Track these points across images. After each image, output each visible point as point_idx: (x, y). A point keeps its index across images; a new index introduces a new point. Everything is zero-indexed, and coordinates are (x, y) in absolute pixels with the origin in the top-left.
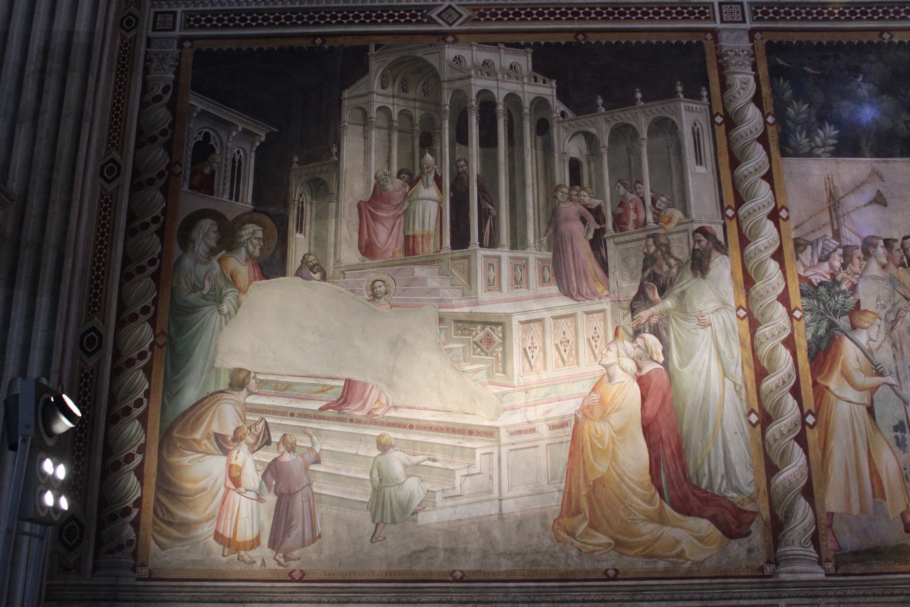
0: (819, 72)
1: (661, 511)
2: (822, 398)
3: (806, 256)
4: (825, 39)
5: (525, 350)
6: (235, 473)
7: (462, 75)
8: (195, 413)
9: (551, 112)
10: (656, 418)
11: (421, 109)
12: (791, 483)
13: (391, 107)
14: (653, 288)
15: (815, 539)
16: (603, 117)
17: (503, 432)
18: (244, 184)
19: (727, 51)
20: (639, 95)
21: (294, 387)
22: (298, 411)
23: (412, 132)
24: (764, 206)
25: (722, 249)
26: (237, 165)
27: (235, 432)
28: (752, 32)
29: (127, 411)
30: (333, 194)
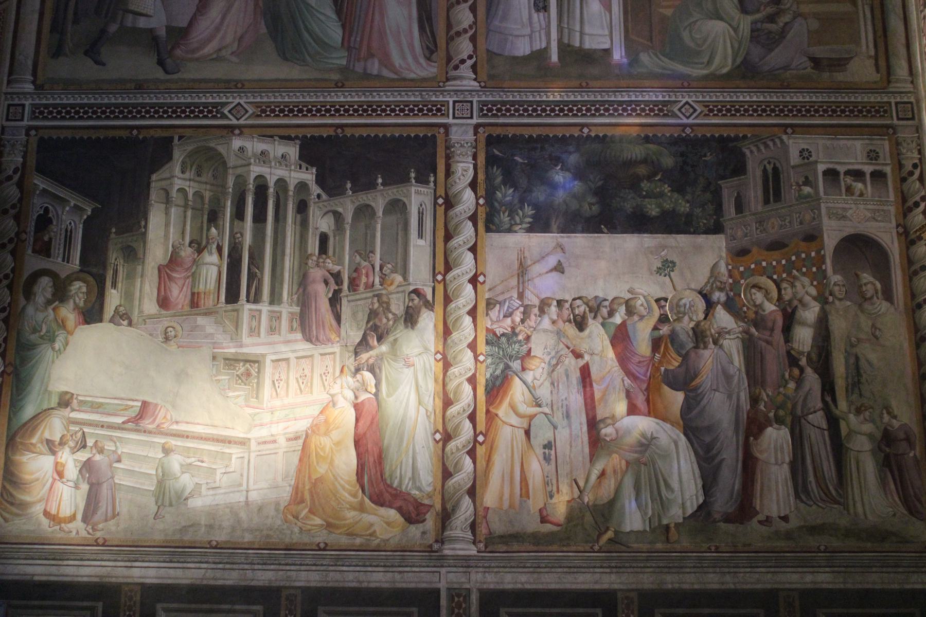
3: (494, 313)
4: (535, 132)
5: (273, 381)
6: (59, 468)
7: (244, 162)
9: (310, 195)
10: (365, 434)
12: (459, 485)
13: (187, 189)
14: (373, 336)
15: (473, 526)
20: (380, 181)
23: (202, 210)
25: (430, 306)
26: (69, 234)
27: (61, 438)
28: (477, 127)
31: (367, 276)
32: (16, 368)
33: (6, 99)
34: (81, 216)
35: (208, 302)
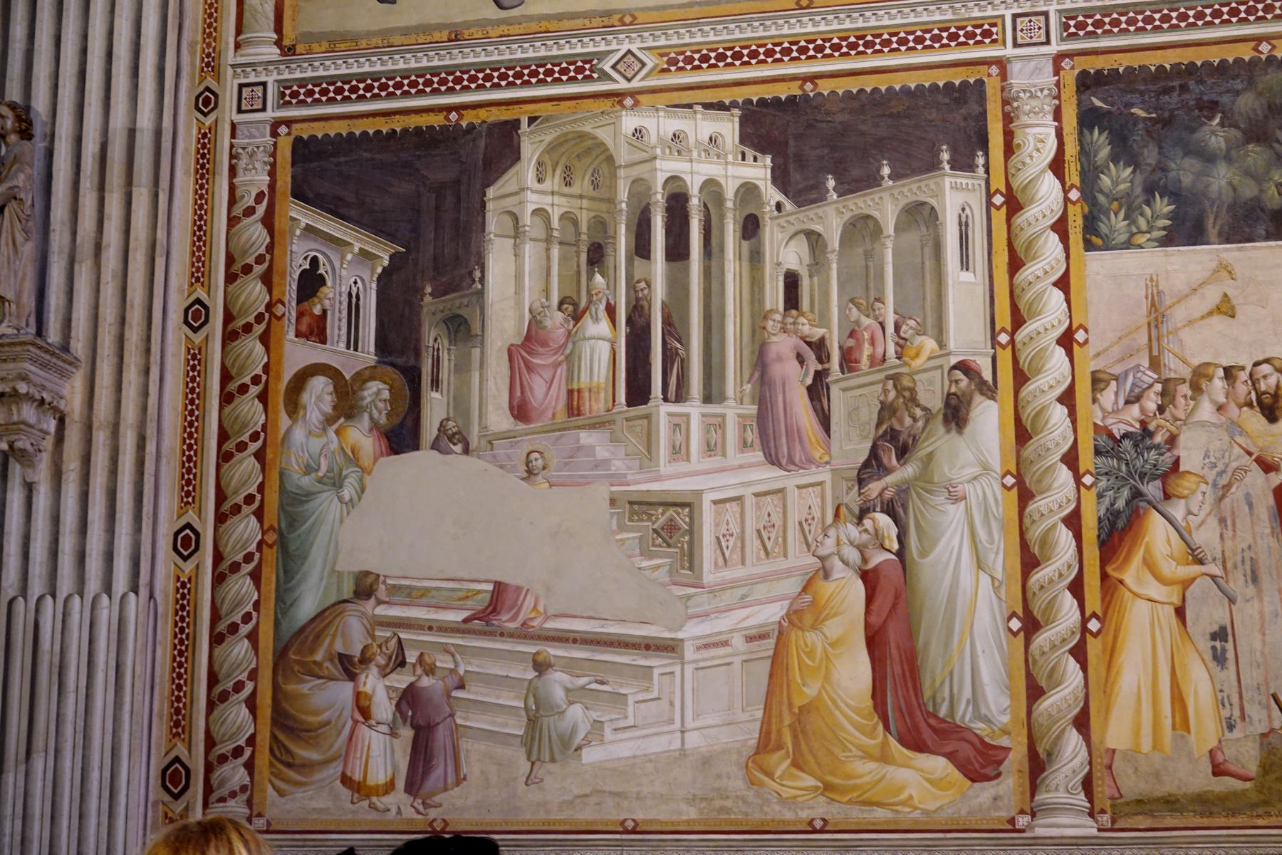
0: (1154, 115)
1: (885, 743)
2: (1112, 595)
3: (1108, 397)
4: (1168, 59)
5: (718, 538)
6: (364, 703)
7: (644, 155)
8: (314, 629)
9: (762, 205)
13: (549, 209)
16: (835, 206)
20: (886, 171)
21: (434, 593)
22: (438, 624)
23: (576, 244)
24: (1053, 326)
25: (989, 390)
26: (354, 300)
28: (1058, 58)
29: (234, 628)
30: (477, 335)
31: (873, 342)
32: (281, 535)
33: (235, 75)
35: (596, 406)
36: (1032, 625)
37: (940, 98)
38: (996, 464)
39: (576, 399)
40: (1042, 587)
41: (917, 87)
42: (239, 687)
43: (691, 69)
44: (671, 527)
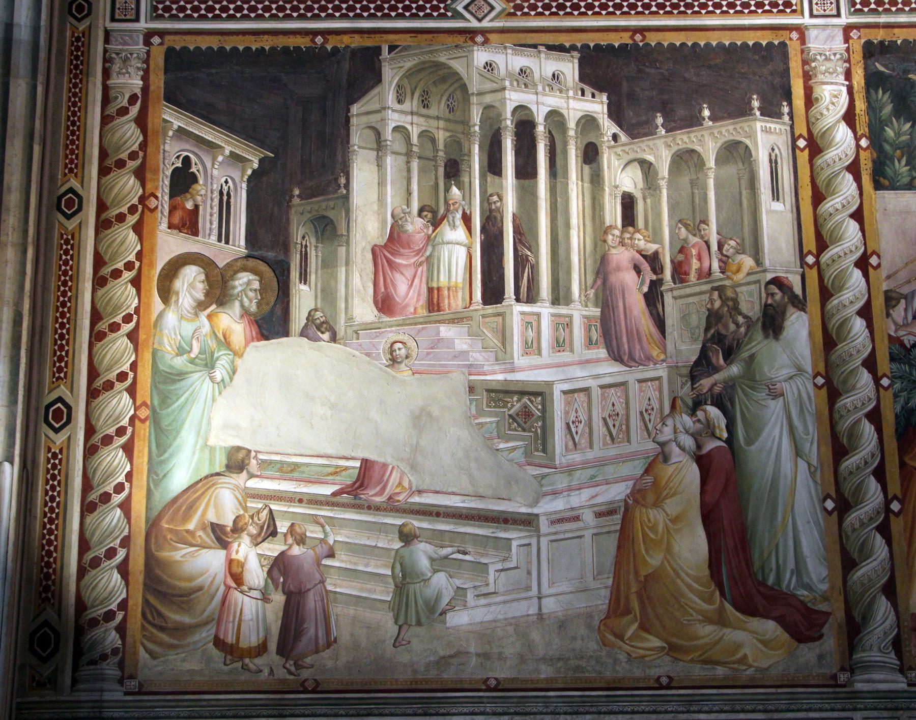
1: (722, 608)
3: (899, 313)
5: (568, 424)
6: (236, 569)
8: (187, 499)
11: (446, 130)
12: (870, 580)
13: (409, 127)
14: (717, 351)
16: (663, 140)
17: (543, 520)
18: (235, 223)
19: (815, 55)
20: (706, 113)
21: (303, 469)
23: (434, 159)
24: (851, 251)
25: (800, 304)
26: (225, 198)
27: (235, 522)
29: (106, 498)
30: (342, 235)
32: (154, 411)
34: (243, 171)
35: (457, 302)
36: (844, 506)
37: (750, 55)
38: (809, 368)
39: (436, 296)
40: (851, 473)
41: (730, 44)
42: (111, 553)
43: (535, 15)
44: (526, 413)
